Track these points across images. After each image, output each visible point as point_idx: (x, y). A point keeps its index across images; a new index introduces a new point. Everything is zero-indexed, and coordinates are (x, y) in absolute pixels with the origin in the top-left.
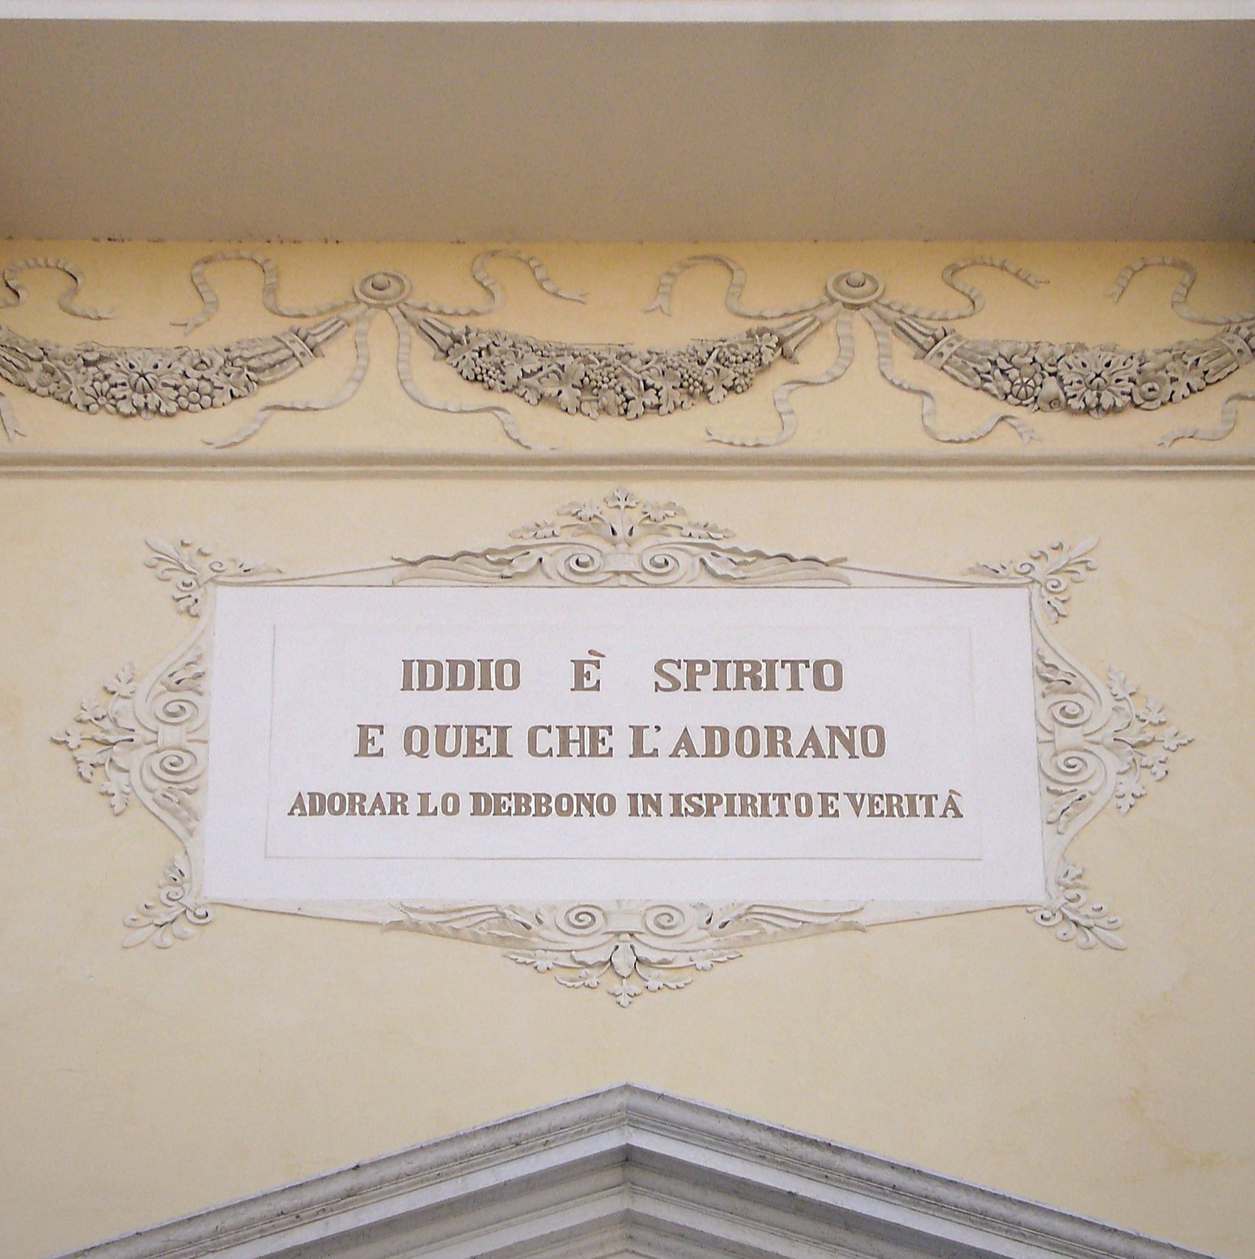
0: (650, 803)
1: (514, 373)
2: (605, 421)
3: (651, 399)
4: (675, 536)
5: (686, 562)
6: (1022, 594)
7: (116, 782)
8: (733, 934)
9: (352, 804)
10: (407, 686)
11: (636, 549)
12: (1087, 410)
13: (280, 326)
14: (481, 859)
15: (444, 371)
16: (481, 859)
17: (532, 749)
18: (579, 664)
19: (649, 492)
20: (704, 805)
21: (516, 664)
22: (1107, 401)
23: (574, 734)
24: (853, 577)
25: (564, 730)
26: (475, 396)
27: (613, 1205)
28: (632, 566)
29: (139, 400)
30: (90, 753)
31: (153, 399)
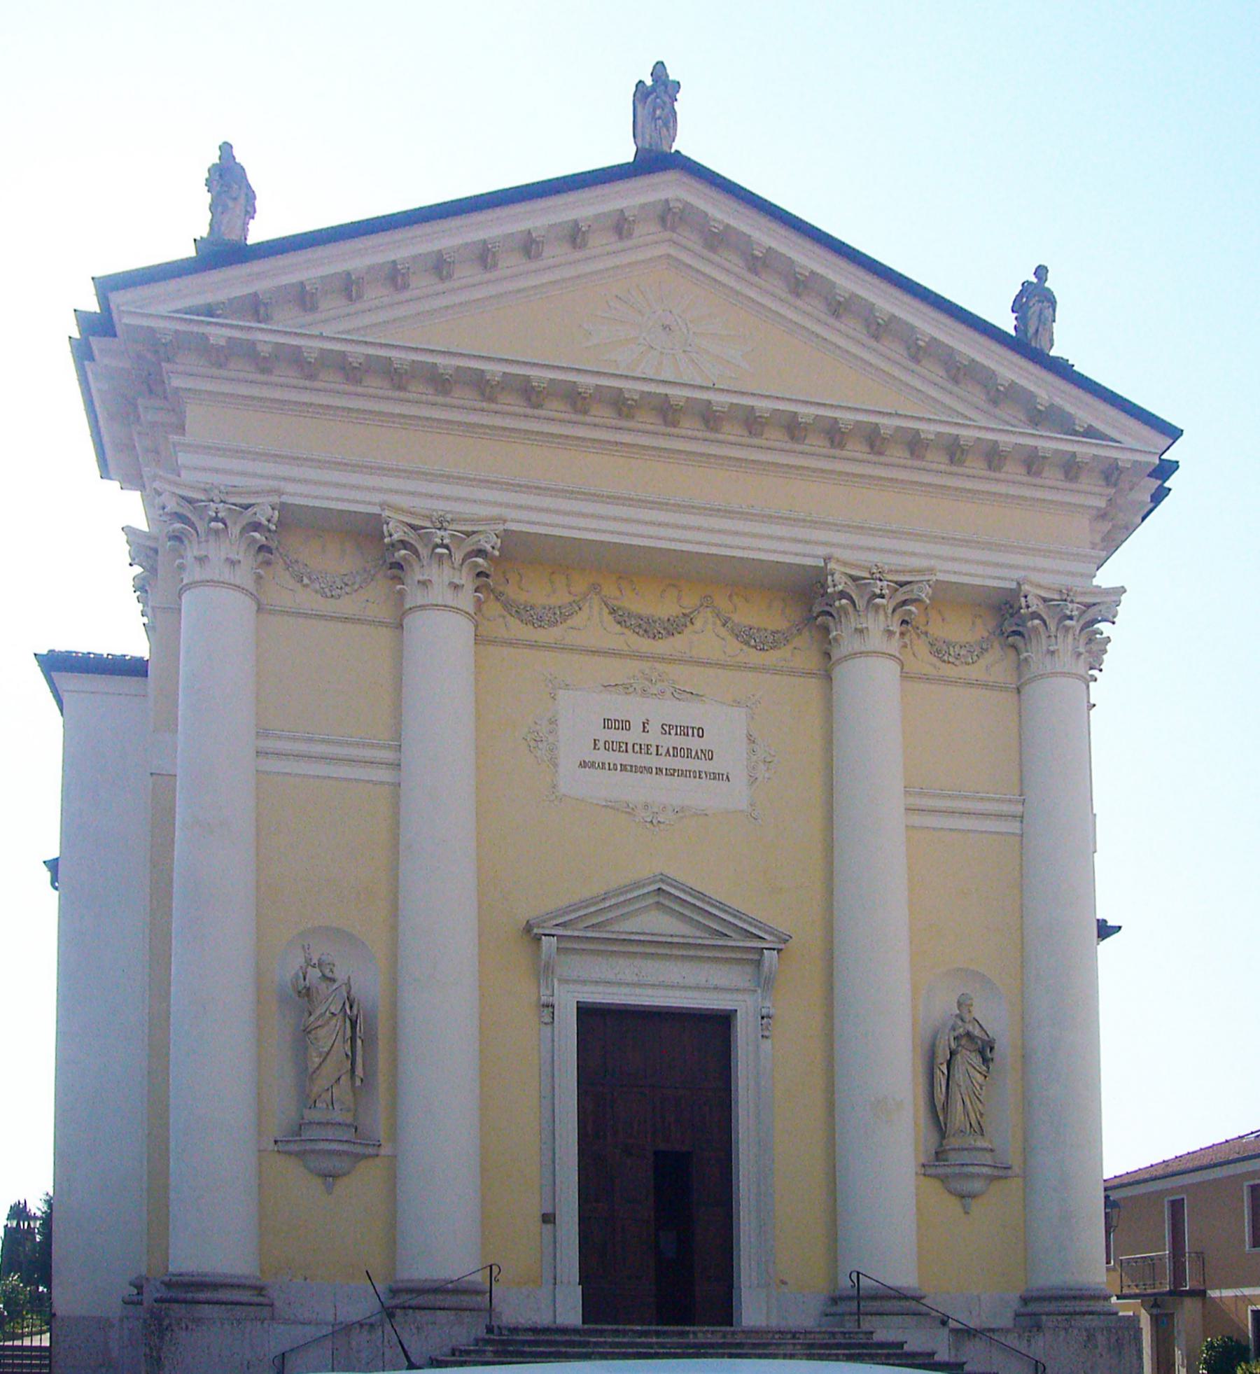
0: (659, 770)
1: (628, 624)
2: (649, 640)
3: (660, 636)
4: (666, 683)
5: (668, 693)
6: (744, 710)
7: (539, 754)
8: (680, 814)
9: (592, 765)
10: (604, 727)
11: (657, 686)
12: (760, 650)
13: (571, 598)
14: (306, 615)
15: (611, 618)
16: (306, 615)
17: (634, 751)
18: (644, 723)
19: (660, 667)
20: (671, 773)
21: (629, 722)
22: (766, 648)
23: (643, 747)
24: (706, 700)
25: (641, 745)
26: (618, 628)
27: (656, 899)
28: (656, 692)
29: (539, 623)
30: (533, 744)
31: (543, 624)
